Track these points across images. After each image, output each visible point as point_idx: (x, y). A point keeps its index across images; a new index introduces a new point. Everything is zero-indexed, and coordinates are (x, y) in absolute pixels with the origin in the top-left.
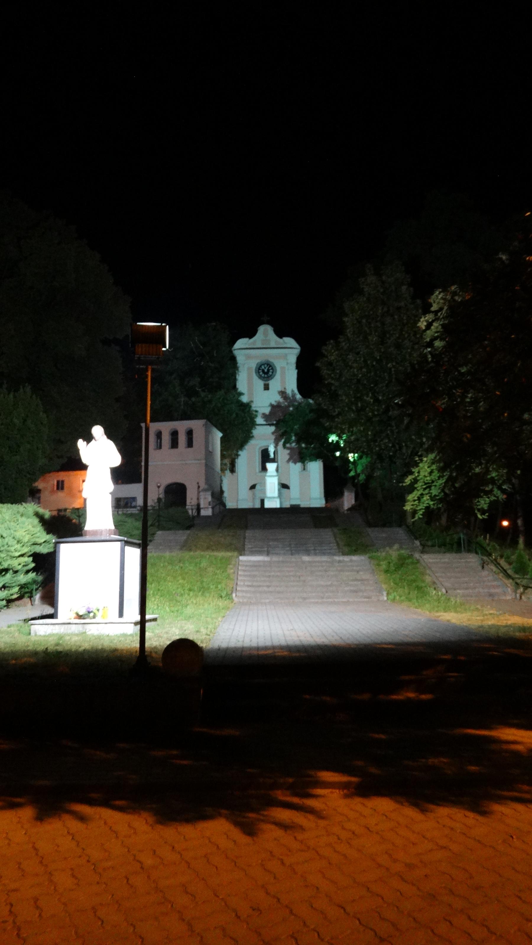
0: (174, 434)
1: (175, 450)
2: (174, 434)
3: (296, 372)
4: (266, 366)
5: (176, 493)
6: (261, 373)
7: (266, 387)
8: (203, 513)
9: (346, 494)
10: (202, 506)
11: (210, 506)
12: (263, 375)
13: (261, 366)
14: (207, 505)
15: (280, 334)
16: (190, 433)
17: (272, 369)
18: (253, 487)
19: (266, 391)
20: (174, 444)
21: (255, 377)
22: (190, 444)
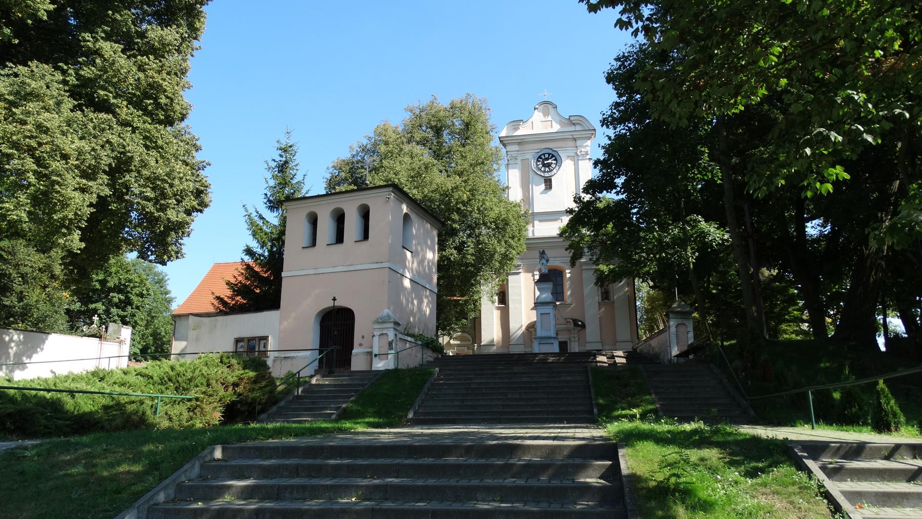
0: (340, 218)
1: (339, 246)
2: (340, 218)
4: (547, 156)
5: (337, 326)
13: (540, 157)
14: (385, 349)
16: (365, 214)
22: (366, 236)
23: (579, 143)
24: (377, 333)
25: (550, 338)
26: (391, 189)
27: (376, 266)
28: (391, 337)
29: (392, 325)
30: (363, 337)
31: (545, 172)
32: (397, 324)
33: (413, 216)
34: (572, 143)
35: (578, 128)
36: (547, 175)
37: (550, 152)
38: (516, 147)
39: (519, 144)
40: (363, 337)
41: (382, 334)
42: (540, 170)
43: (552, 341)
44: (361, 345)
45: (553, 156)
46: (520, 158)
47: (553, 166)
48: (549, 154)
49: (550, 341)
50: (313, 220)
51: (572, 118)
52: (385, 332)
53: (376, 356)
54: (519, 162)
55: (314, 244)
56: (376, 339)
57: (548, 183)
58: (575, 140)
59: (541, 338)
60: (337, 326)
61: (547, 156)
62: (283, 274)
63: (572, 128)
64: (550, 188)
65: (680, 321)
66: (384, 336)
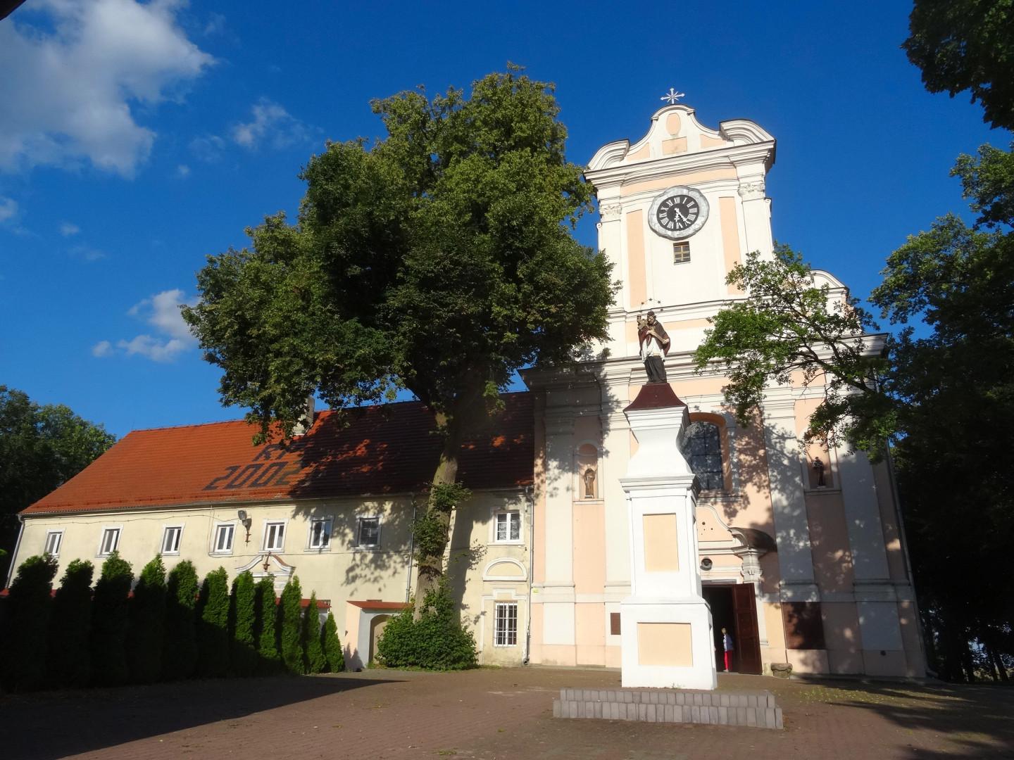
3: (763, 209)
6: (665, 221)
12: (671, 225)
13: (664, 204)
15: (710, 118)
17: (696, 205)
23: (742, 170)
31: (675, 229)
35: (738, 142)
36: (676, 234)
37: (685, 192)
38: (616, 191)
39: (623, 182)
42: (665, 227)
45: (690, 199)
46: (624, 211)
47: (692, 217)
48: (682, 197)
54: (623, 216)
57: (682, 251)
58: (733, 164)
61: (677, 201)
63: (730, 144)
64: (688, 260)
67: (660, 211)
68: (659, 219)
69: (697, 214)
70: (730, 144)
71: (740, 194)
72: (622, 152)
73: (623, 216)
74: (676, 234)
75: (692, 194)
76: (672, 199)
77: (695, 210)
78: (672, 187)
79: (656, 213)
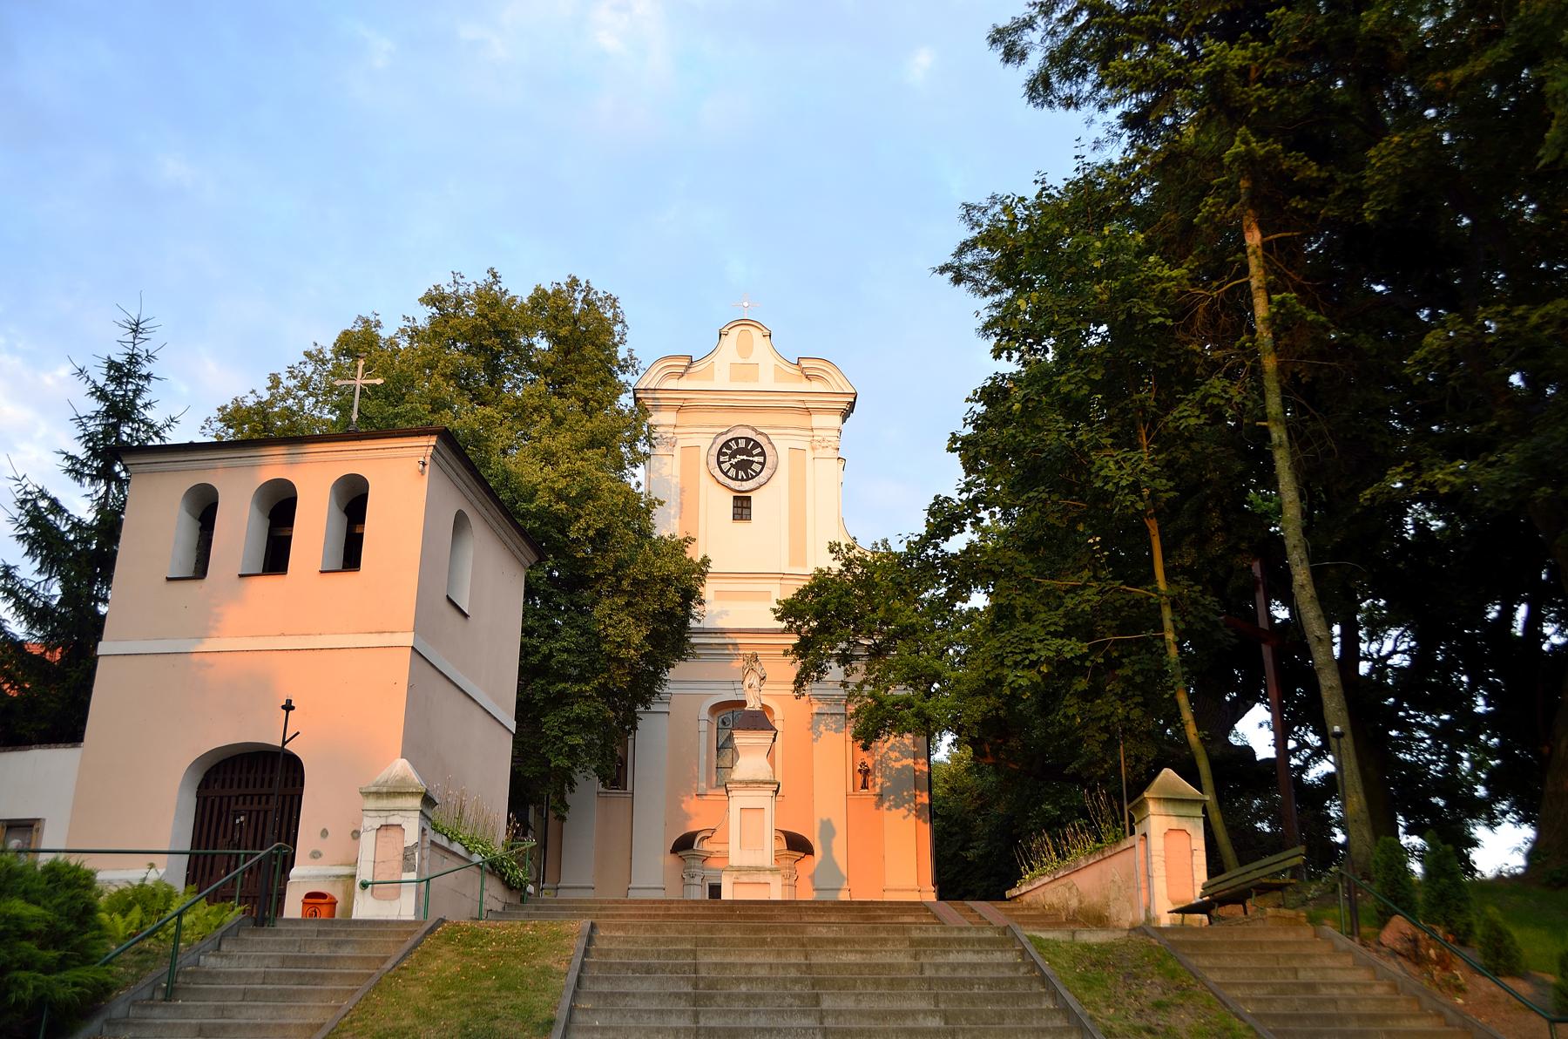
2: (280, 508)
4: (742, 444)
7: (742, 508)
8: (365, 908)
9: (1158, 821)
10: (365, 873)
11: (413, 876)
12: (732, 473)
13: (726, 445)
14: (393, 870)
16: (353, 501)
17: (763, 454)
18: (684, 844)
19: (741, 525)
20: (276, 559)
21: (705, 479)
22: (351, 557)
23: (818, 420)
24: (371, 822)
25: (758, 869)
26: (433, 440)
27: (375, 640)
28: (412, 834)
29: (416, 802)
30: (325, 833)
31: (736, 479)
32: (428, 801)
33: (476, 524)
34: (801, 420)
35: (816, 386)
37: (751, 434)
40: (325, 833)
41: (387, 826)
42: (725, 474)
43: (768, 877)
44: (316, 855)
45: (757, 445)
46: (680, 443)
47: (757, 467)
48: (748, 440)
49: (762, 878)
50: (205, 508)
51: (804, 364)
52: (392, 820)
53: (364, 885)
55: (201, 569)
56: (367, 840)
57: (742, 508)
59: (739, 869)
60: (249, 797)
61: (742, 444)
62: (102, 648)
63: (806, 386)
65: (1174, 823)
66: (392, 833)
67: (720, 453)
68: (719, 463)
69: (763, 464)
70: (806, 386)
71: (813, 449)
72: (682, 370)
73: (677, 451)
74: (735, 485)
75: (759, 439)
76: (736, 439)
77: (761, 459)
78: (741, 425)
79: (715, 451)
